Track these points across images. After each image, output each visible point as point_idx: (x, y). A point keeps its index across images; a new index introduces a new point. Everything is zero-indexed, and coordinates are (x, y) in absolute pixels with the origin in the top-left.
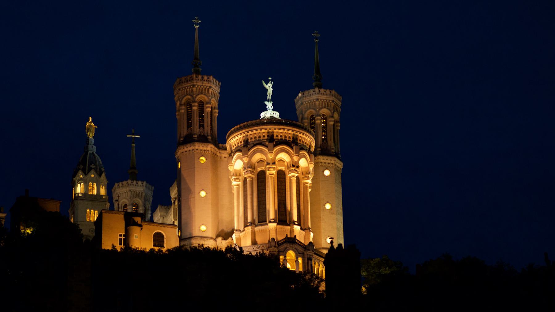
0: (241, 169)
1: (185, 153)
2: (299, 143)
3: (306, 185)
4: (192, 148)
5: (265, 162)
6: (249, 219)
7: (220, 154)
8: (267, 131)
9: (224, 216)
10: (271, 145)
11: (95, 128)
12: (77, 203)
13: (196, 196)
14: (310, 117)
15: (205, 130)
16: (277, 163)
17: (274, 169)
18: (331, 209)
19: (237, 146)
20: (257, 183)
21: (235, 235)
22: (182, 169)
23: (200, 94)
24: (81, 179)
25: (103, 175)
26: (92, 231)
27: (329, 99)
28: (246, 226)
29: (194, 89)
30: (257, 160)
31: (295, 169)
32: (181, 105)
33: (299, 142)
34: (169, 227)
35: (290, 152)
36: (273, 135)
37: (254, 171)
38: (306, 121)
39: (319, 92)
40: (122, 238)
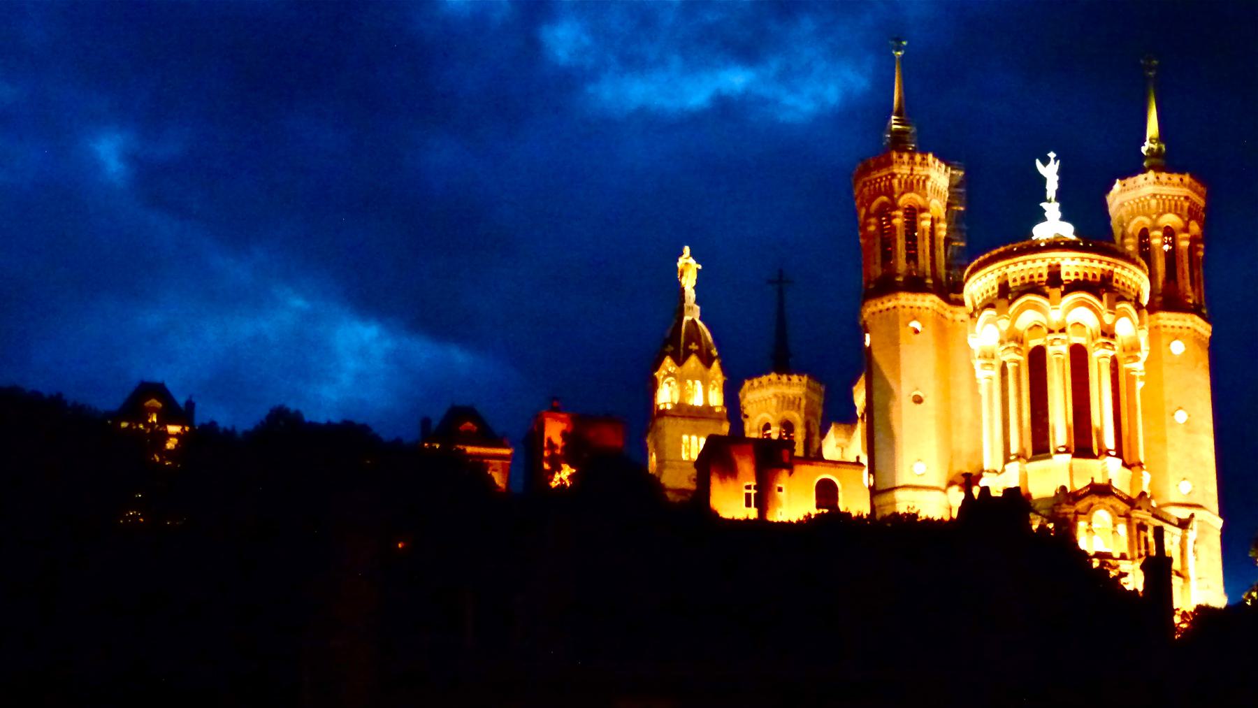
3: (1132, 373)
6: (1014, 449)
10: (1056, 292)
11: (697, 269)
16: (1069, 329)
17: (1063, 342)
19: (985, 297)
22: (873, 348)
24: (670, 374)
25: (716, 364)
28: (1007, 460)
29: (895, 182)
32: (868, 215)
33: (1115, 284)
37: (1023, 348)
39: (1156, 180)
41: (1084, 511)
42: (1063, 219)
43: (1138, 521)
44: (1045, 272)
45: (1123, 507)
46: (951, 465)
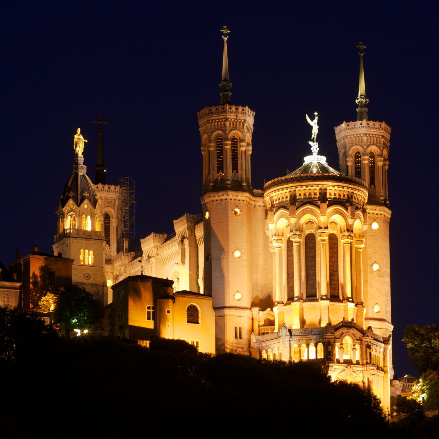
0: (284, 228)
1: (215, 202)
2: (354, 202)
5: (315, 224)
6: (297, 293)
7: (254, 202)
8: (319, 188)
10: (325, 205)
11: (85, 142)
12: (69, 241)
13: (230, 256)
14: (355, 154)
15: (239, 173)
20: (305, 248)
21: (278, 309)
22: (212, 222)
23: (233, 129)
26: (87, 277)
27: (379, 134)
28: (291, 299)
30: (306, 221)
31: (350, 234)
33: (354, 200)
34: (204, 299)
35: (345, 213)
36: (326, 193)
37: (302, 235)
38: (351, 159)
39: (367, 125)
40: (150, 311)
41: (339, 337)
42: (320, 153)
43: (366, 343)
44: (318, 192)
45: (358, 334)
46: (253, 292)
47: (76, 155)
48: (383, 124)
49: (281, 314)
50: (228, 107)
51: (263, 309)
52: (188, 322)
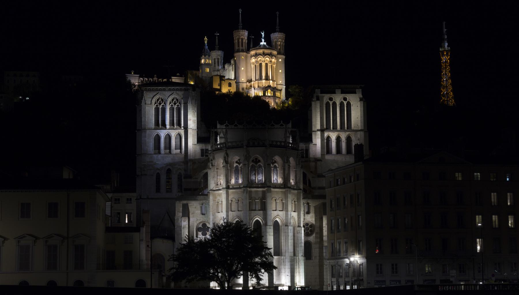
4: (239, 54)
6: (257, 79)
9: (249, 75)
10: (264, 55)
13: (241, 69)
18: (281, 72)
24: (203, 58)
28: (256, 80)
32: (236, 39)
42: (264, 42)
45: (272, 89)
46: (247, 78)
47: (204, 43)
48: (283, 33)
49: (254, 84)
50: (240, 30)
51: (249, 83)
52: (229, 86)
